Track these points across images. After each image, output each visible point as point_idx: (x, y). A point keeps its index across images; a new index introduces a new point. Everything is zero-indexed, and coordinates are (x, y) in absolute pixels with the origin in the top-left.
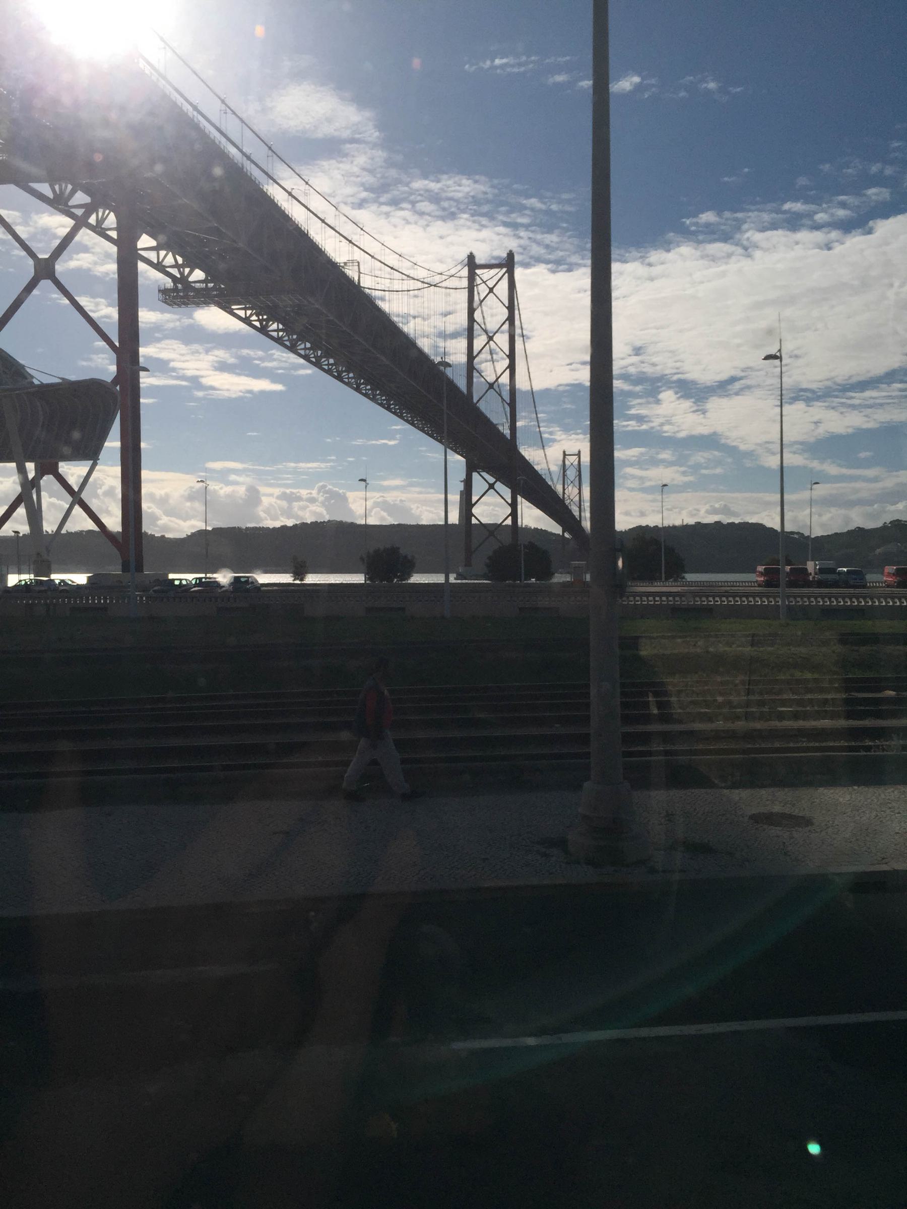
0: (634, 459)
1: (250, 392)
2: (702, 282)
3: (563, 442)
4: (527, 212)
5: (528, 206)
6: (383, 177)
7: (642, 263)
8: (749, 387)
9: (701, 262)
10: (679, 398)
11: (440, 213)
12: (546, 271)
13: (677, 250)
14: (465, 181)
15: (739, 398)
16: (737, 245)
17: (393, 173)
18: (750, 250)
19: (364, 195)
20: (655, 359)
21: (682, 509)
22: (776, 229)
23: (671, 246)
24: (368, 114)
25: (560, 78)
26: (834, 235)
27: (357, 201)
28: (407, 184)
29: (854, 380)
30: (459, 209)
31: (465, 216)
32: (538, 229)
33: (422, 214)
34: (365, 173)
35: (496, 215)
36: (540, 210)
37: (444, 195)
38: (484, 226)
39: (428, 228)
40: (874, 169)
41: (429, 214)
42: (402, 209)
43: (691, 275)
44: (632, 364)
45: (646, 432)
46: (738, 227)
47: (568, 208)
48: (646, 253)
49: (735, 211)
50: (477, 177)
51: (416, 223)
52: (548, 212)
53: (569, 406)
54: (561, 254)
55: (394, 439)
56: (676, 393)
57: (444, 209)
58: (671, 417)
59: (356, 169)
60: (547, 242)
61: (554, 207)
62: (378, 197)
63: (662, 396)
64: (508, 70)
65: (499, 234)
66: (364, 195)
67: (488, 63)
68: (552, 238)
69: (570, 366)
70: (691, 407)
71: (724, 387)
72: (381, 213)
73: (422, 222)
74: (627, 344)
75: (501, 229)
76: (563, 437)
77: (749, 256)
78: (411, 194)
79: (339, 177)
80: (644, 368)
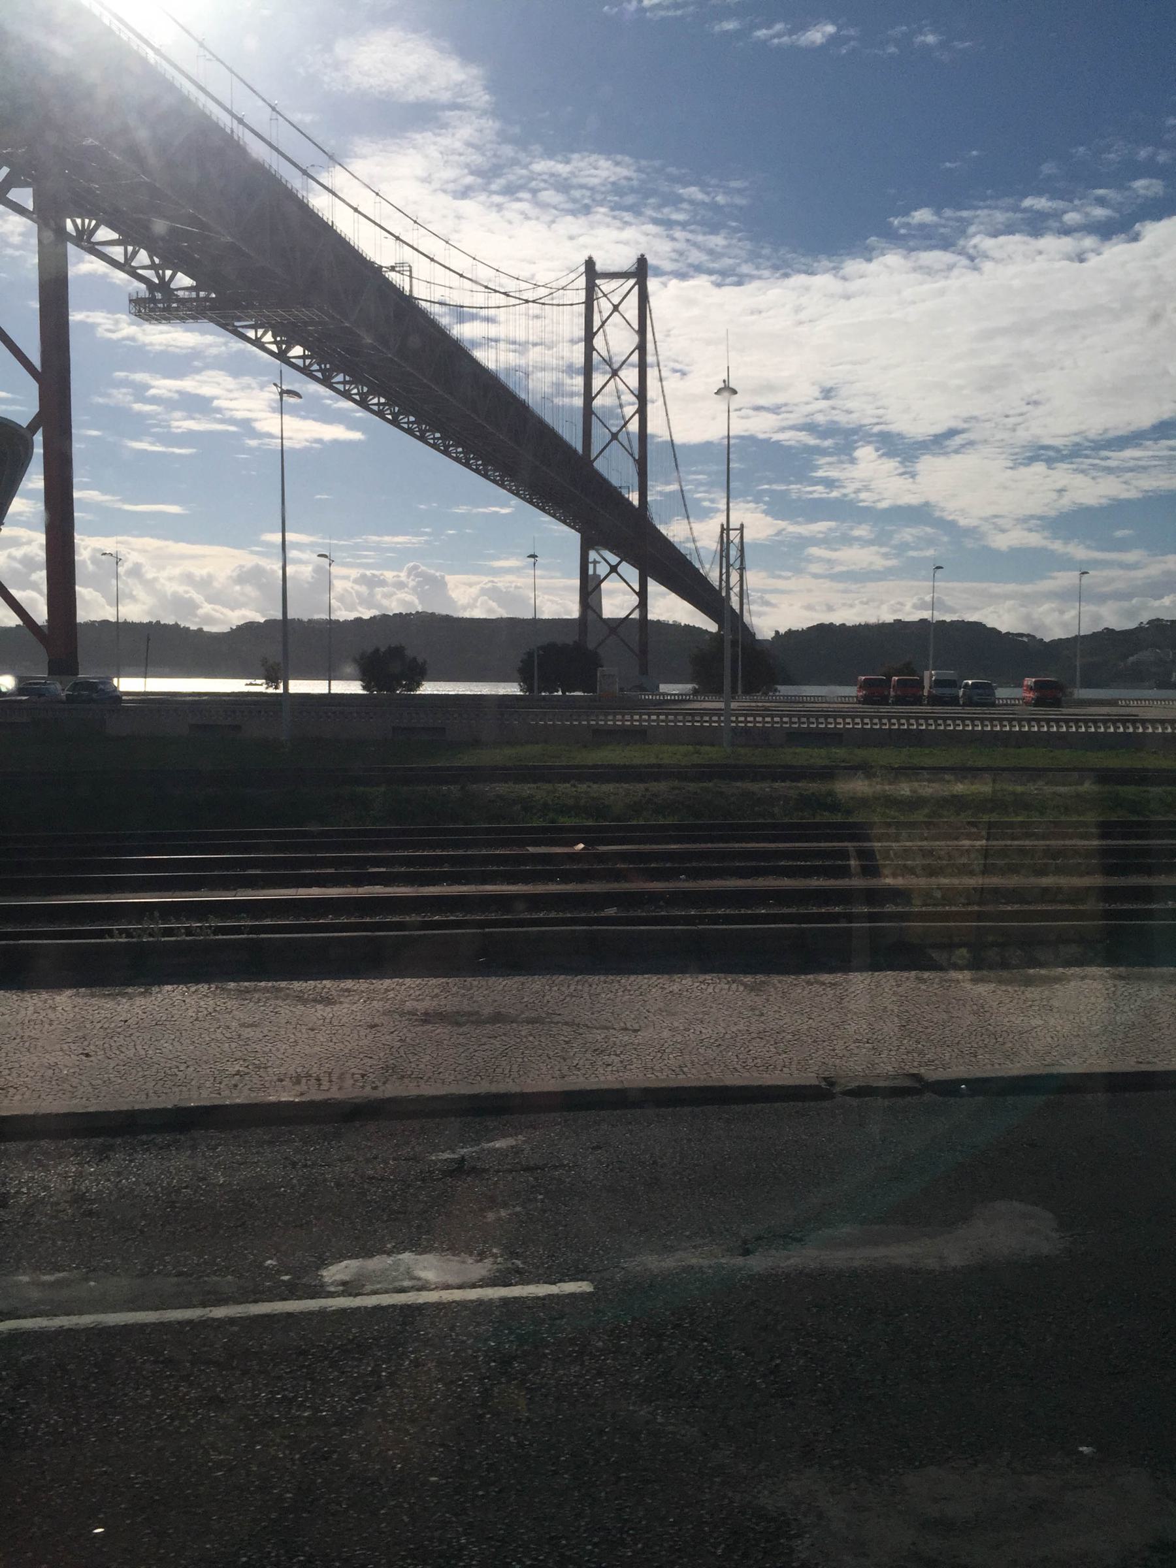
0: (821, 536)
1: (319, 441)
2: (914, 303)
4: (685, 206)
5: (686, 197)
6: (495, 155)
7: (835, 276)
8: (971, 443)
9: (913, 276)
10: (880, 457)
11: (570, 206)
12: (709, 284)
13: (881, 259)
15: (958, 458)
16: (960, 254)
17: (508, 150)
18: (977, 261)
19: (469, 180)
20: (850, 405)
21: (882, 602)
22: (1012, 233)
23: (874, 253)
24: (474, 71)
25: (730, 25)
26: (1089, 242)
28: (526, 167)
29: (1111, 434)
30: (594, 200)
31: (602, 210)
32: (699, 228)
34: (470, 150)
37: (575, 181)
38: (627, 223)
39: (554, 225)
40: (1143, 154)
41: (555, 208)
42: (519, 200)
43: (899, 292)
44: (820, 411)
46: (962, 229)
47: (741, 201)
49: (959, 207)
50: (619, 157)
51: (537, 218)
52: (715, 207)
54: (731, 261)
56: (877, 450)
57: (574, 201)
58: (870, 481)
59: (458, 145)
60: (711, 245)
61: (721, 199)
62: (489, 183)
63: (858, 453)
64: (663, 13)
65: (648, 235)
66: (469, 180)
68: (718, 241)
69: (738, 412)
70: (896, 468)
71: (939, 443)
72: (492, 205)
74: (813, 384)
75: (651, 228)
77: (976, 269)
79: (437, 155)
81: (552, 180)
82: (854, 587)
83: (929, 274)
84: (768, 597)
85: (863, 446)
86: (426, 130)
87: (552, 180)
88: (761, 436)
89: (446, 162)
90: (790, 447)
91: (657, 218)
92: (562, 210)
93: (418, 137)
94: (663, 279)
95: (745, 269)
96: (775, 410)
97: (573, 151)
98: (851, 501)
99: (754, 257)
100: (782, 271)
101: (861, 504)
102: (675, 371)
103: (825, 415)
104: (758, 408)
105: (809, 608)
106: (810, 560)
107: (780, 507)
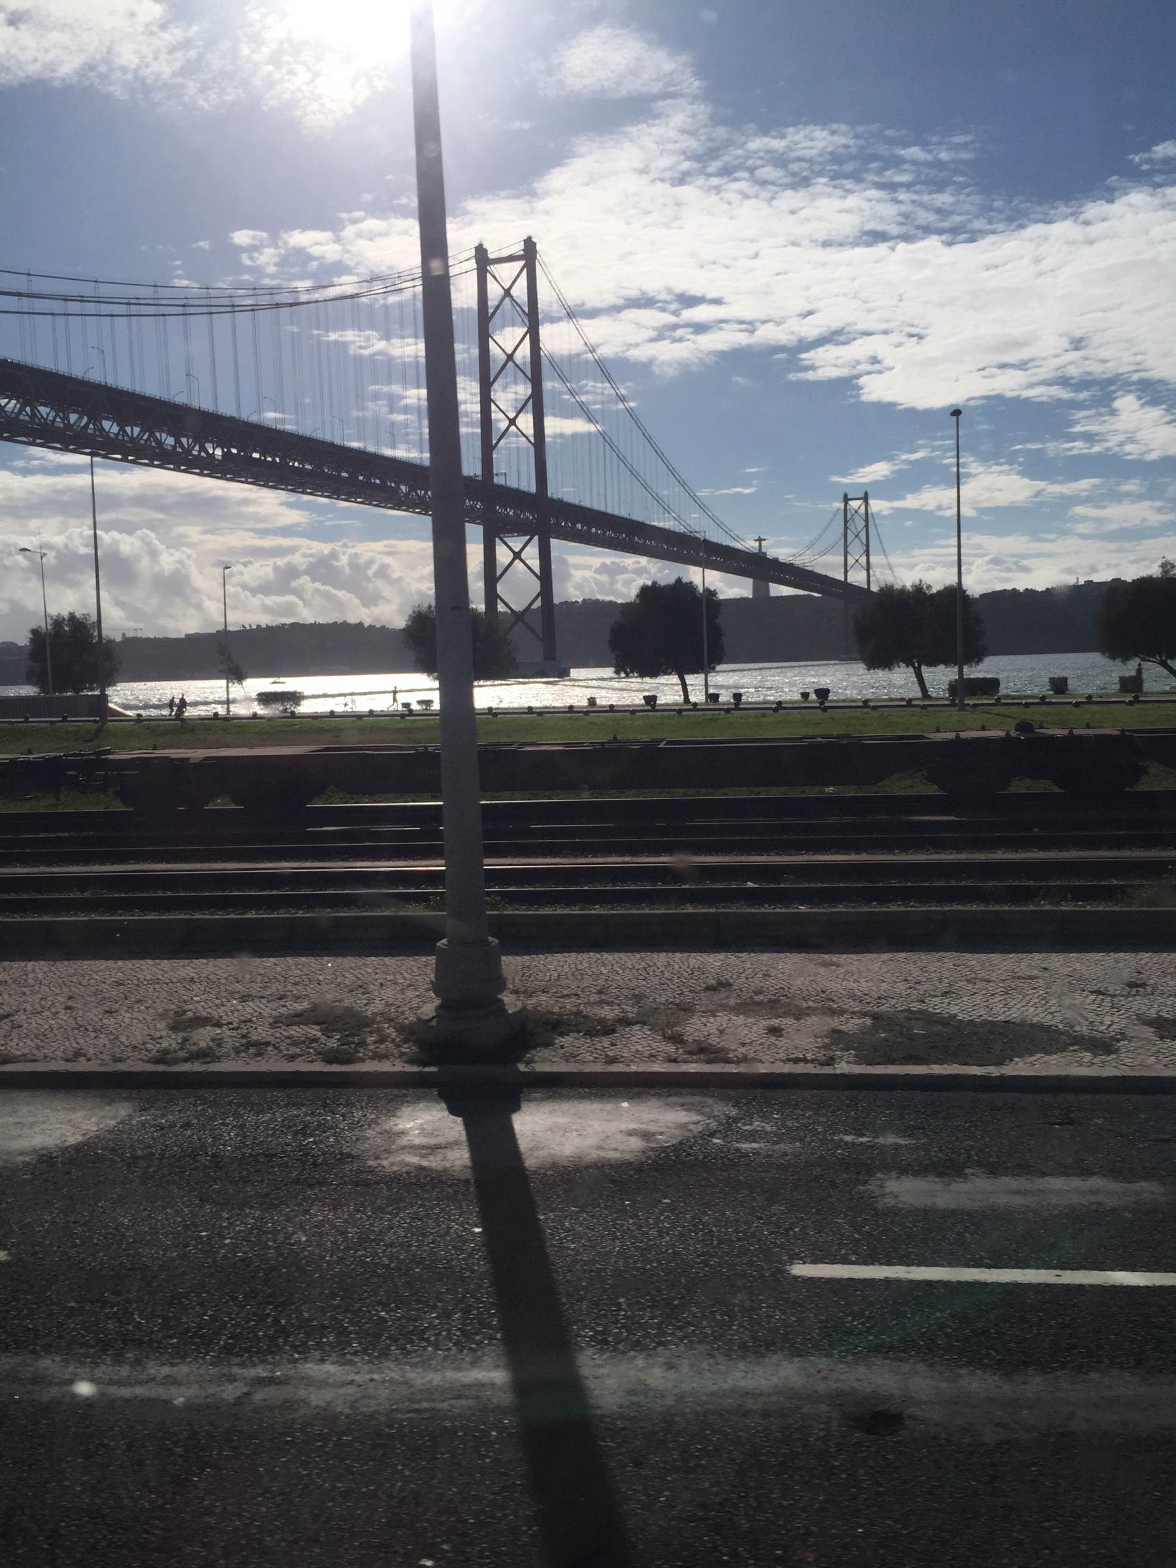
0: (1085, 494)
3: (981, 476)
4: (906, 166)
6: (711, 140)
7: (1075, 221)
9: (1161, 213)
10: (1143, 405)
13: (1125, 199)
17: (722, 132)
19: (686, 165)
20: (1104, 354)
24: (684, 58)
28: (742, 146)
30: (813, 172)
31: (823, 180)
32: (923, 187)
33: (763, 183)
34: (685, 136)
37: (792, 155)
39: (775, 202)
41: (774, 184)
42: (737, 180)
43: (1147, 232)
44: (1071, 363)
45: (1099, 455)
47: (965, 155)
48: (1080, 207)
50: (835, 126)
51: (757, 197)
52: (939, 165)
53: (985, 427)
54: (958, 219)
55: (751, 486)
56: (1139, 398)
57: (794, 174)
58: (1135, 432)
60: (938, 204)
61: (944, 156)
62: (705, 167)
63: (1117, 404)
66: (686, 165)
68: (944, 199)
70: (1162, 416)
74: (1061, 335)
75: (874, 193)
76: (981, 469)
78: (748, 158)
79: (654, 146)
80: (1089, 365)
82: (1127, 545)
84: (1025, 562)
85: (1123, 396)
88: (1010, 394)
90: (1043, 403)
91: (879, 183)
93: (633, 130)
94: (891, 243)
95: (978, 224)
96: (1022, 366)
97: (788, 125)
98: (1115, 454)
99: (985, 211)
100: (1016, 223)
101: (1127, 457)
102: (912, 336)
104: (1003, 366)
105: (1069, 571)
106: (1075, 520)
107: (1037, 467)
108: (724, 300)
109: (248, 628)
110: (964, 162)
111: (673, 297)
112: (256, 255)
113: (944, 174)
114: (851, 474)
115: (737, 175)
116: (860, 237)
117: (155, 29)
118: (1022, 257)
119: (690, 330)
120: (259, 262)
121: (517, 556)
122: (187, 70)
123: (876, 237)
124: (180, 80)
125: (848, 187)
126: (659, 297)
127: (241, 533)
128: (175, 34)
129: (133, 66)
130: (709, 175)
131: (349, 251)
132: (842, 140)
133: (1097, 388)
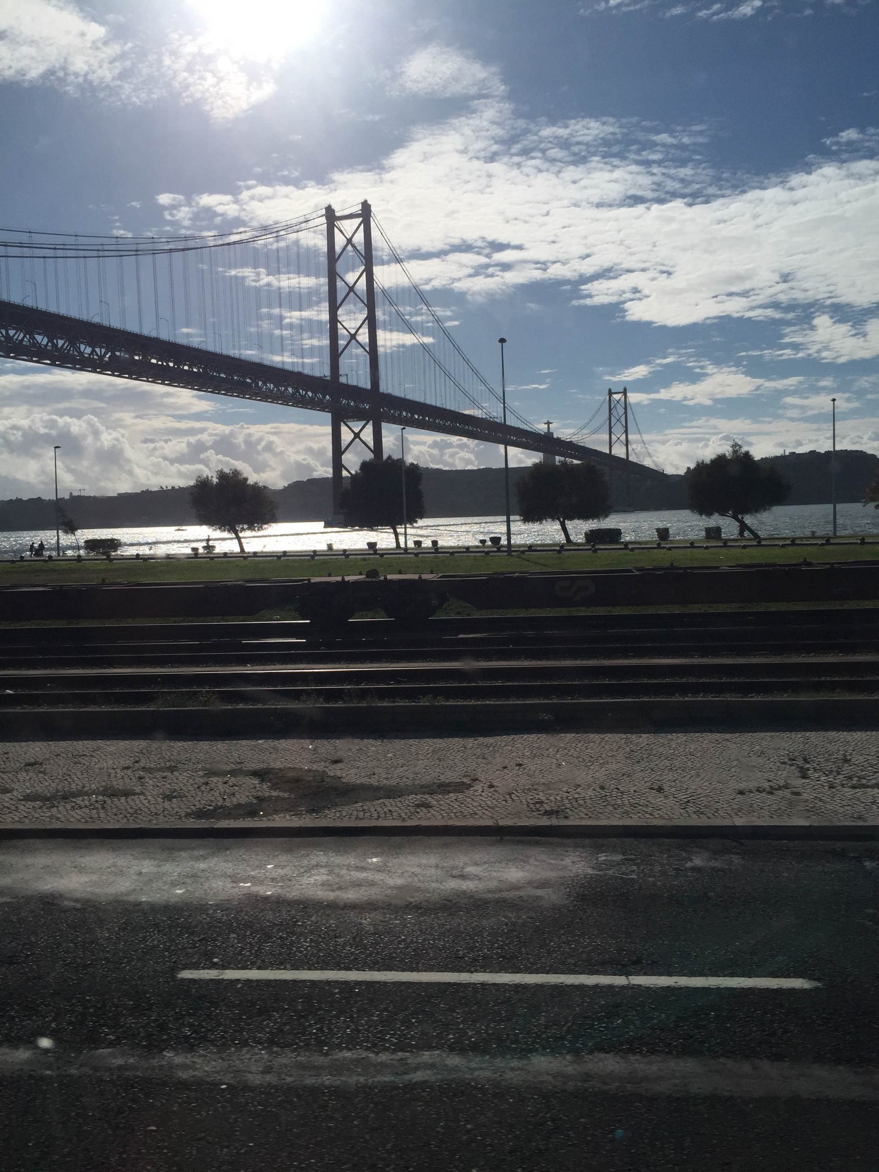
0: (792, 388)
1: (404, 346)
3: (715, 375)
4: (658, 148)
6: (513, 128)
7: (783, 188)
9: (846, 182)
10: (835, 322)
12: (682, 205)
13: (819, 171)
14: (593, 124)
17: (521, 123)
19: (495, 148)
20: (806, 285)
24: (493, 69)
27: (488, 155)
28: (536, 134)
30: (589, 152)
32: (671, 163)
33: (553, 161)
34: (494, 126)
35: (627, 155)
36: (673, 146)
37: (574, 140)
38: (615, 166)
39: (562, 175)
41: (560, 161)
42: (533, 158)
43: (836, 195)
44: (782, 292)
47: (701, 140)
50: (605, 119)
51: (548, 170)
52: (683, 147)
54: (698, 186)
55: (546, 383)
56: (832, 317)
57: (575, 154)
59: (485, 124)
60: (682, 175)
61: (686, 140)
62: (510, 149)
63: (816, 322)
66: (495, 148)
67: (603, 4)
68: (686, 172)
69: (715, 299)
70: (850, 331)
73: (555, 169)
74: (774, 272)
75: (634, 168)
76: (715, 370)
78: (541, 142)
79: (471, 133)
81: (556, 141)
83: (860, 179)
85: (819, 316)
86: (462, 116)
87: (556, 141)
88: (736, 315)
89: (477, 137)
91: (640, 160)
92: (566, 162)
93: (456, 122)
94: (647, 205)
95: (711, 190)
96: (745, 294)
99: (717, 181)
100: (739, 189)
101: (824, 361)
102: (663, 272)
103: (786, 295)
104: (730, 294)
105: (781, 445)
106: (785, 407)
107: (755, 368)
108: (525, 247)
109: (165, 489)
110: (700, 145)
111: (485, 244)
112: (175, 212)
113: (685, 154)
114: (620, 374)
115: (533, 154)
116: (625, 200)
117: (100, 45)
118: (743, 215)
119: (498, 268)
120: (177, 218)
121: (357, 435)
122: (124, 75)
123: (635, 200)
124: (119, 83)
125: (615, 163)
126: (475, 244)
127: (163, 418)
128: (115, 49)
129: (83, 73)
130: (513, 155)
131: (245, 210)
132: (611, 129)
133: (800, 310)
